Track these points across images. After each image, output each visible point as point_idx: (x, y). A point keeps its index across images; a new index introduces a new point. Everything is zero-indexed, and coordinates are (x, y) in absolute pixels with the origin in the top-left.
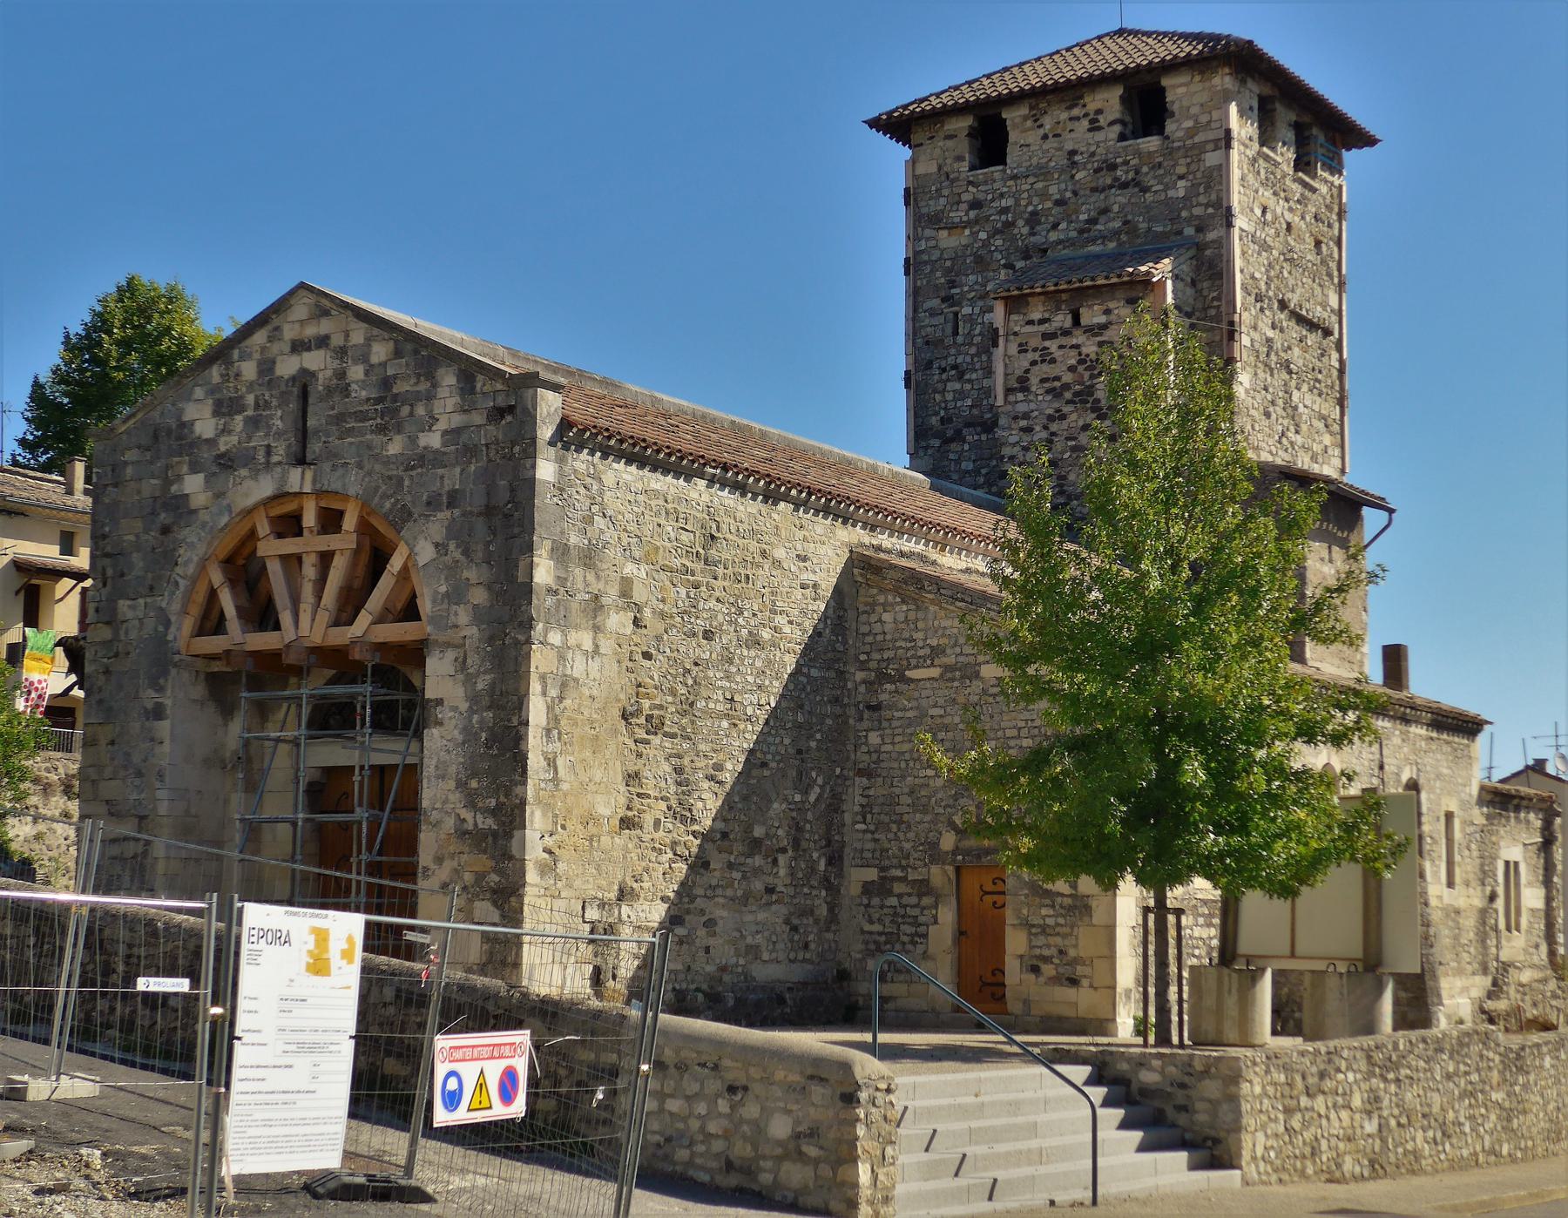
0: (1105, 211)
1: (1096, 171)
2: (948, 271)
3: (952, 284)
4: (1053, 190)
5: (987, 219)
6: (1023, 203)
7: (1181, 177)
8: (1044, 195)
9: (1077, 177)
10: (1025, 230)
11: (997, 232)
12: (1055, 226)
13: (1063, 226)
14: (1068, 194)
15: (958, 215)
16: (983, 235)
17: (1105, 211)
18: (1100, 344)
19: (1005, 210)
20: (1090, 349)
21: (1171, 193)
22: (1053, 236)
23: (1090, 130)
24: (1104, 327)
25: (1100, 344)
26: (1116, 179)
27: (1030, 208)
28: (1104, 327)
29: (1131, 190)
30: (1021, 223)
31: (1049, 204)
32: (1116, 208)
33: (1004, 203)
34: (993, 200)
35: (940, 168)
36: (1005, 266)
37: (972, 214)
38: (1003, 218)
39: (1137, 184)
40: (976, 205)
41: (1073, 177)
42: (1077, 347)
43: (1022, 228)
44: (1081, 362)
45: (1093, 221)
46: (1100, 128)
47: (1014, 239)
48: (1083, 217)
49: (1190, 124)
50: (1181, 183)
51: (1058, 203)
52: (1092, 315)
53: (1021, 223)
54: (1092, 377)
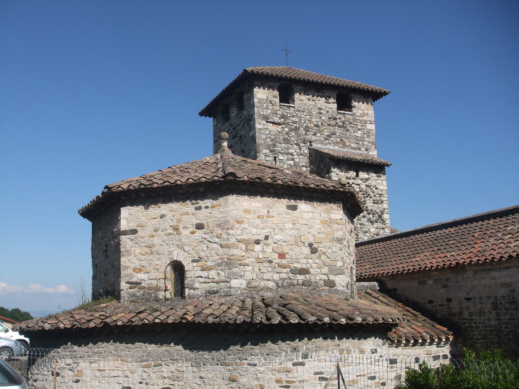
0: (334, 134)
1: (330, 118)
2: (272, 140)
3: (275, 146)
4: (314, 120)
5: (288, 124)
6: (303, 121)
7: (359, 130)
8: (310, 121)
9: (322, 118)
10: (304, 132)
11: (291, 130)
12: (315, 134)
13: (318, 134)
14: (320, 124)
15: (276, 120)
16: (286, 129)
17: (334, 134)
18: (367, 186)
19: (294, 122)
20: (363, 186)
21: (356, 134)
22: (314, 138)
23: (326, 103)
24: (367, 180)
25: (367, 186)
26: (337, 123)
27: (305, 125)
28: (367, 180)
29: (342, 129)
30: (302, 129)
31: (312, 125)
32: (338, 134)
33: (294, 119)
34: (290, 117)
35: (267, 98)
36: (296, 144)
37: (282, 120)
38: (295, 125)
39: (344, 128)
40: (283, 116)
41: (321, 118)
42: (358, 185)
43: (302, 131)
44: (360, 191)
45: (329, 136)
46: (329, 103)
47: (299, 135)
48: (326, 134)
49: (361, 112)
50: (359, 132)
51: (315, 126)
52: (363, 175)
53: (302, 129)
54: (364, 197)
